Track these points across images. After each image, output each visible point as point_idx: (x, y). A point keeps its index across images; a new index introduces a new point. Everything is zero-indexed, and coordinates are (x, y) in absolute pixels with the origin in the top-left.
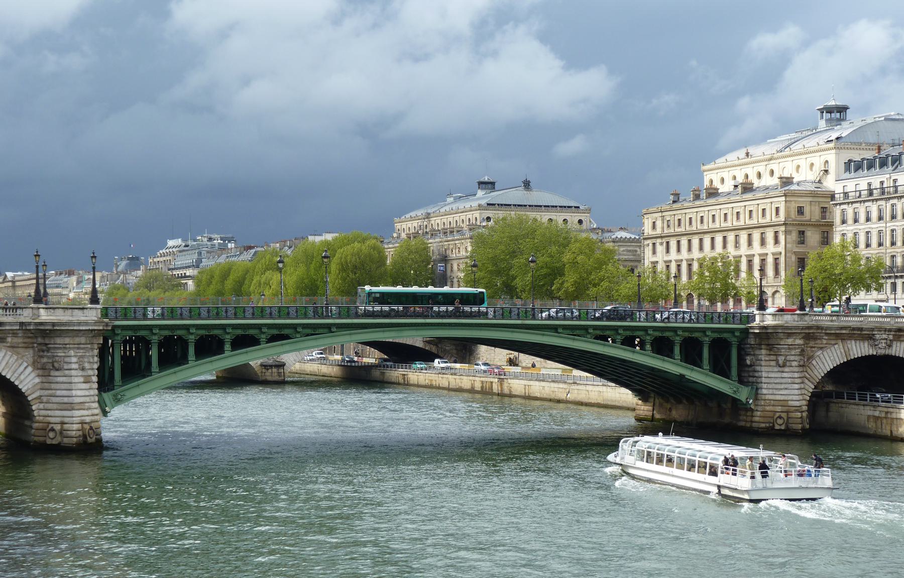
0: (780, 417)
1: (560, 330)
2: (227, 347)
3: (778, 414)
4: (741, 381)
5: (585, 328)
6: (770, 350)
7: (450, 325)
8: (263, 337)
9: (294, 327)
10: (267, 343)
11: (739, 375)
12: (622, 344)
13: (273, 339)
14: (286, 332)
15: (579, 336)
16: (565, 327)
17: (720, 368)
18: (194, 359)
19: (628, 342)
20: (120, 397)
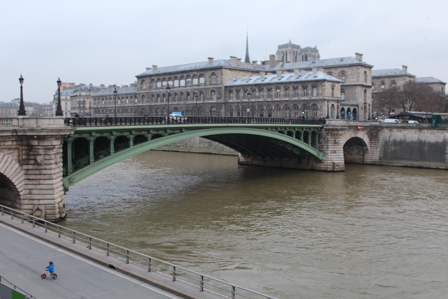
0: (337, 165)
1: (269, 129)
2: (131, 143)
3: (336, 165)
4: (319, 150)
5: (276, 128)
6: (332, 136)
7: (231, 127)
8: (149, 136)
9: (165, 130)
10: (151, 139)
11: (319, 148)
12: (287, 135)
13: (155, 137)
14: (161, 132)
15: (273, 131)
16: (272, 128)
17: (313, 145)
18: (114, 152)
19: (290, 134)
20: (72, 180)
